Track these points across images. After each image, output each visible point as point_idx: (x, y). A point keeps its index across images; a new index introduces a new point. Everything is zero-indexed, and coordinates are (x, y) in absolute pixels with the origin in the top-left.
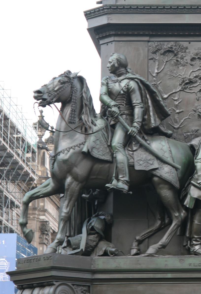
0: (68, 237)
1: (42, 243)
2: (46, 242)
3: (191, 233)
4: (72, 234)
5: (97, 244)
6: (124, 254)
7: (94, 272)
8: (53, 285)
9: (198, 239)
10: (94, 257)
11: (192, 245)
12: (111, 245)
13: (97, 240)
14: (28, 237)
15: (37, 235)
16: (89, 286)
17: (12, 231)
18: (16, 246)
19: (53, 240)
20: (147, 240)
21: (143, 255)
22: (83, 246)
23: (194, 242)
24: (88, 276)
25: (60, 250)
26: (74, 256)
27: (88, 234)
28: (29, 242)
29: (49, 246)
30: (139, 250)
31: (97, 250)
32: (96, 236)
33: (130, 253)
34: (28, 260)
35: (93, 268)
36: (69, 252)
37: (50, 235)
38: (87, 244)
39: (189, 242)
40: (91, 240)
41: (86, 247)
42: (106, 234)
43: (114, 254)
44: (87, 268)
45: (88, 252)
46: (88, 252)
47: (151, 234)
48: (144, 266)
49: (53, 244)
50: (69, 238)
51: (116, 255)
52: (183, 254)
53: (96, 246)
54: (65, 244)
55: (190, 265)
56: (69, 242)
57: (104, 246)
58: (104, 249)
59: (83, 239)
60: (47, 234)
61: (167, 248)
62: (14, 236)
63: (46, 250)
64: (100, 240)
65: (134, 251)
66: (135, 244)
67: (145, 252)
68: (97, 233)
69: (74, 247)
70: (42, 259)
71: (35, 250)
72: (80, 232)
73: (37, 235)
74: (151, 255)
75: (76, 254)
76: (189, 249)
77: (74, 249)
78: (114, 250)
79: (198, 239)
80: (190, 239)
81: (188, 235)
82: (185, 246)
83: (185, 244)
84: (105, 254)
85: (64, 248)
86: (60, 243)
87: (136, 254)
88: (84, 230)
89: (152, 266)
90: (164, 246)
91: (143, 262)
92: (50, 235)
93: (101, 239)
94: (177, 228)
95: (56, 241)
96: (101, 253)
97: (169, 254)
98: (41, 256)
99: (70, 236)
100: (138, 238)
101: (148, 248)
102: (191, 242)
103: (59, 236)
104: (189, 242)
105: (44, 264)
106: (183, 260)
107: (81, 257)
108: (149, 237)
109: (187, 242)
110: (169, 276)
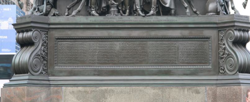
0: (38, 6)
1: (27, 10)
2: (29, 9)
3: (91, 5)
4: (40, 4)
5: (51, 10)
6: (62, 15)
7: (49, 24)
8: (32, 30)
9: (94, 8)
10: (49, 16)
11: (91, 11)
12: (57, 10)
13: (51, 8)
14: (21, 6)
15: (25, 6)
16: (47, 32)
17: (14, 4)
18: (16, 12)
19: (31, 8)
20: (72, 8)
21: (70, 16)
22: (44, 11)
23: (92, 9)
24: (47, 26)
25: (35, 13)
26: (41, 16)
27: (47, 5)
28: (21, 9)
29: (30, 11)
30: (68, 13)
31: (50, 13)
32: (50, 5)
33: (65, 14)
34: (21, 18)
35: (49, 22)
36: (39, 14)
37: (30, 6)
38: (46, 10)
39: (90, 9)
40: (48, 8)
41: (46, 12)
42: (54, 5)
43: (58, 15)
44: (46, 22)
45: (47, 14)
46: (47, 14)
47: (73, 5)
48: (71, 22)
49: (32, 10)
50: (39, 7)
51: (59, 16)
52: (87, 15)
53: (50, 11)
54: (37, 10)
55: (91, 21)
56: (38, 9)
57: (53, 11)
58: (53, 13)
59: (44, 7)
60: (29, 6)
61: (81, 12)
62: (15, 6)
63: (28, 13)
64: (52, 8)
65: (66, 14)
66: (67, 10)
67: (71, 14)
68: (51, 4)
69: (41, 11)
70: (27, 17)
71: (24, 13)
72: (43, 4)
73: (25, 6)
74: (74, 16)
75: (41, 15)
76: (90, 12)
77: (41, 12)
78: (58, 13)
79: (94, 8)
80: (91, 7)
81: (89, 5)
82: (88, 11)
83: (88, 10)
84: (54, 15)
85: (37, 11)
86: (35, 9)
87: (68, 15)
88: (45, 2)
89: (74, 22)
90: (79, 11)
91: (71, 19)
92: (30, 6)
93: (52, 7)
94: (85, 2)
95: (33, 8)
96: (52, 15)
97: (81, 15)
98: (26, 16)
99: (39, 6)
100: (68, 7)
101: (72, 12)
102: (91, 9)
103: (34, 6)
104: (90, 9)
105: (28, 20)
106: (87, 18)
107: (44, 16)
108: (73, 6)
109: (89, 9)
110: (82, 26)
